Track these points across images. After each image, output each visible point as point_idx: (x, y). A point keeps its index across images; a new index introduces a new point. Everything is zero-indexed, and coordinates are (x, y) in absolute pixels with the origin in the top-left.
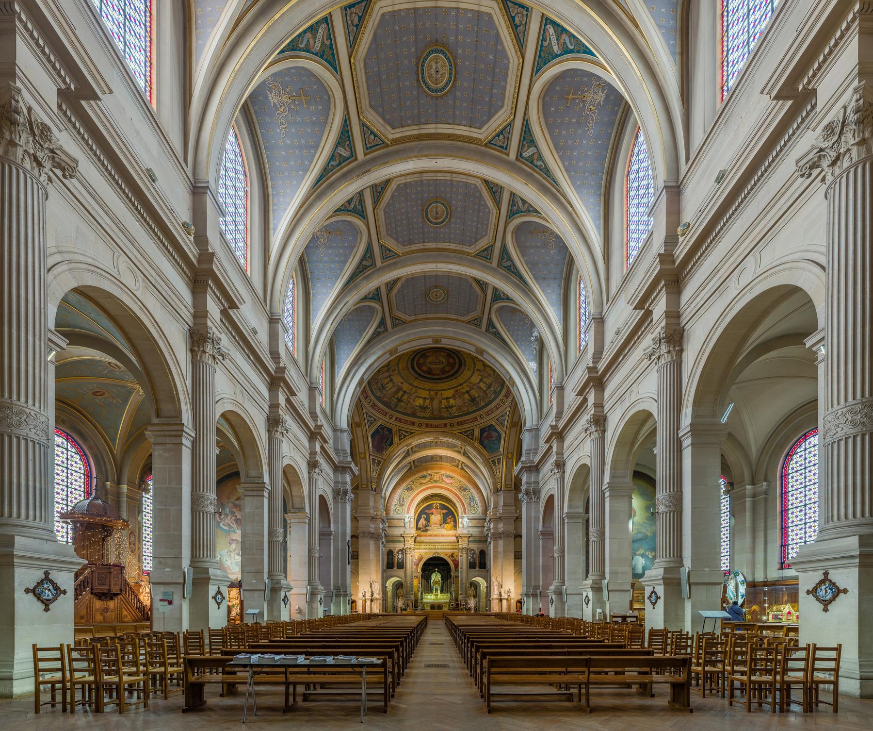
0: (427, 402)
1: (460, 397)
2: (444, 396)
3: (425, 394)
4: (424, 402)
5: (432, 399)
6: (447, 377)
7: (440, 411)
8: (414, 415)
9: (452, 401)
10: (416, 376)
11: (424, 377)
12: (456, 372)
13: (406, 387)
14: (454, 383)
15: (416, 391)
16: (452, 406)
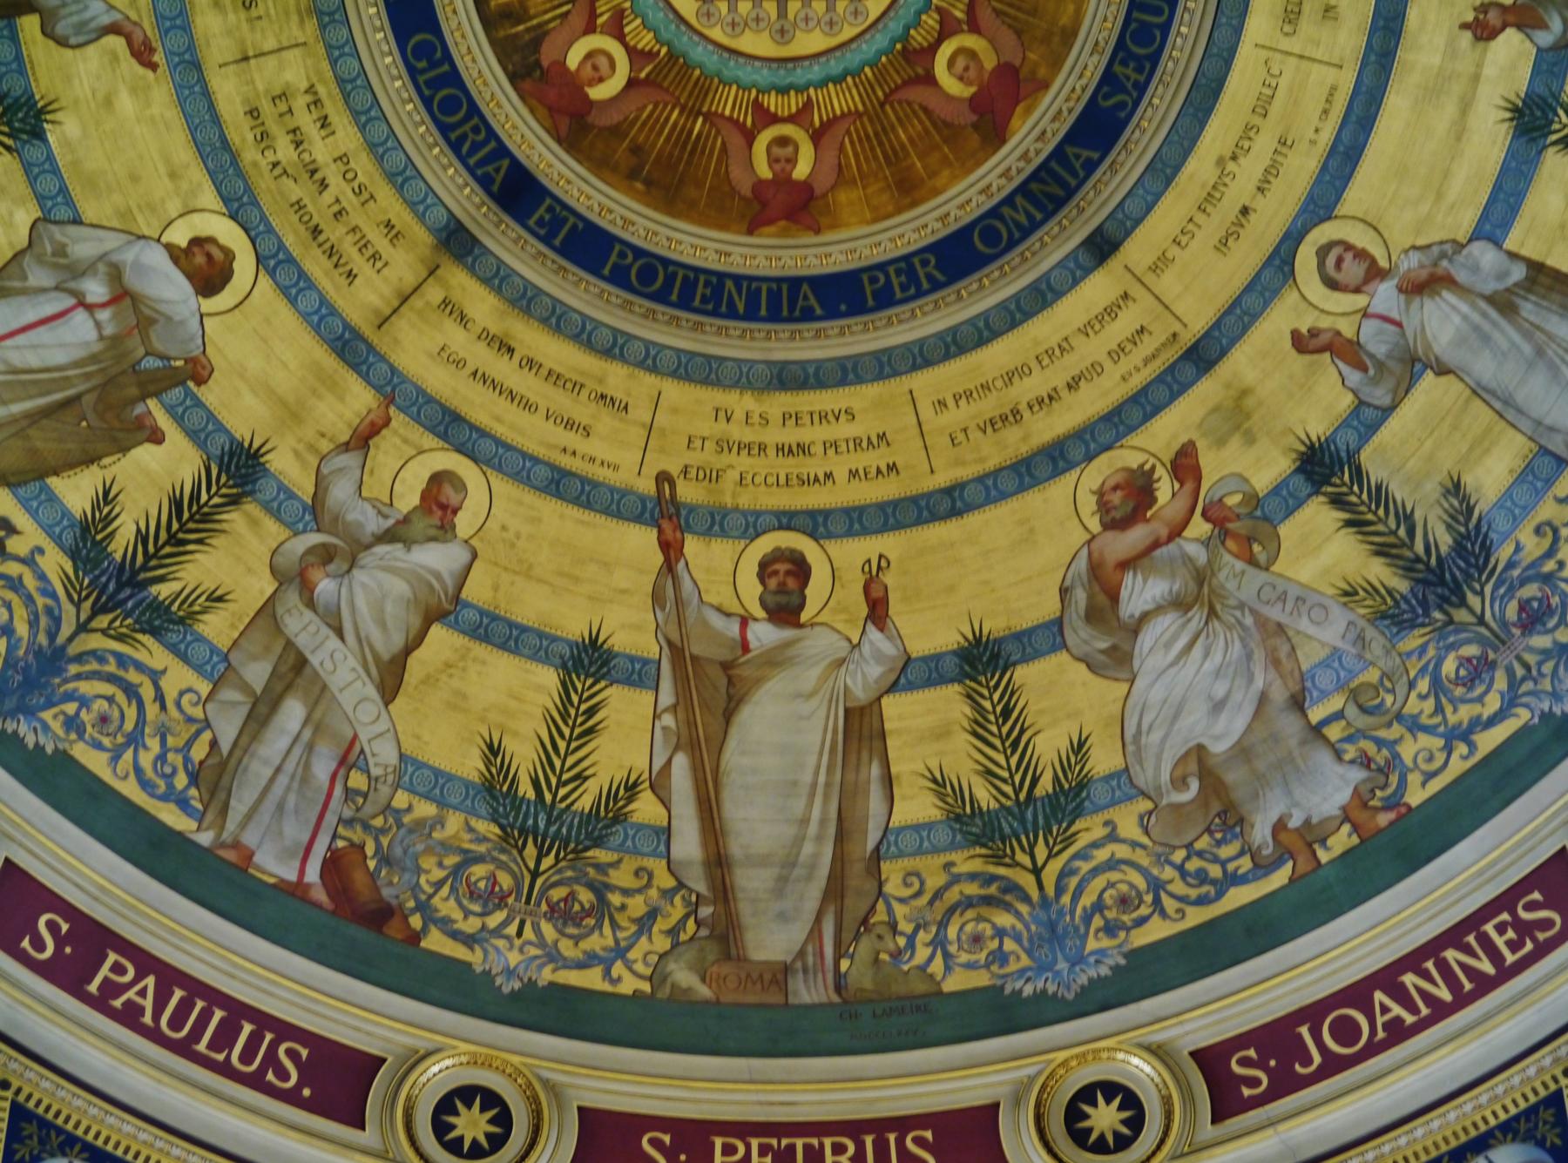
0: (629, 732)
1: (1199, 597)
2: (931, 630)
3: (598, 580)
4: (575, 722)
5: (710, 690)
6: (957, 257)
7: (850, 887)
8: (356, 920)
9: (1062, 701)
10: (457, 191)
11: (586, 246)
12: (1099, 128)
13: (256, 359)
14: (1078, 342)
15: (439, 501)
16: (1072, 797)
